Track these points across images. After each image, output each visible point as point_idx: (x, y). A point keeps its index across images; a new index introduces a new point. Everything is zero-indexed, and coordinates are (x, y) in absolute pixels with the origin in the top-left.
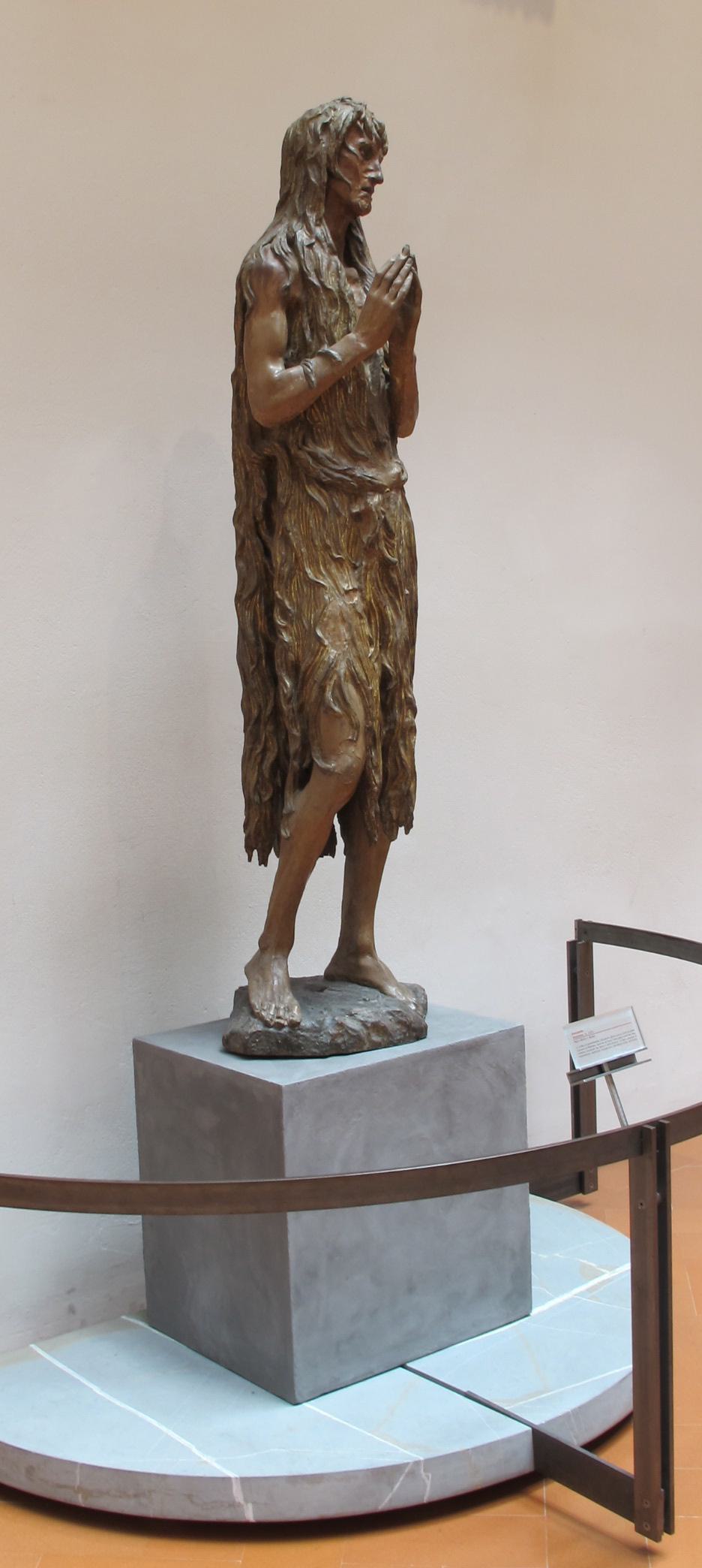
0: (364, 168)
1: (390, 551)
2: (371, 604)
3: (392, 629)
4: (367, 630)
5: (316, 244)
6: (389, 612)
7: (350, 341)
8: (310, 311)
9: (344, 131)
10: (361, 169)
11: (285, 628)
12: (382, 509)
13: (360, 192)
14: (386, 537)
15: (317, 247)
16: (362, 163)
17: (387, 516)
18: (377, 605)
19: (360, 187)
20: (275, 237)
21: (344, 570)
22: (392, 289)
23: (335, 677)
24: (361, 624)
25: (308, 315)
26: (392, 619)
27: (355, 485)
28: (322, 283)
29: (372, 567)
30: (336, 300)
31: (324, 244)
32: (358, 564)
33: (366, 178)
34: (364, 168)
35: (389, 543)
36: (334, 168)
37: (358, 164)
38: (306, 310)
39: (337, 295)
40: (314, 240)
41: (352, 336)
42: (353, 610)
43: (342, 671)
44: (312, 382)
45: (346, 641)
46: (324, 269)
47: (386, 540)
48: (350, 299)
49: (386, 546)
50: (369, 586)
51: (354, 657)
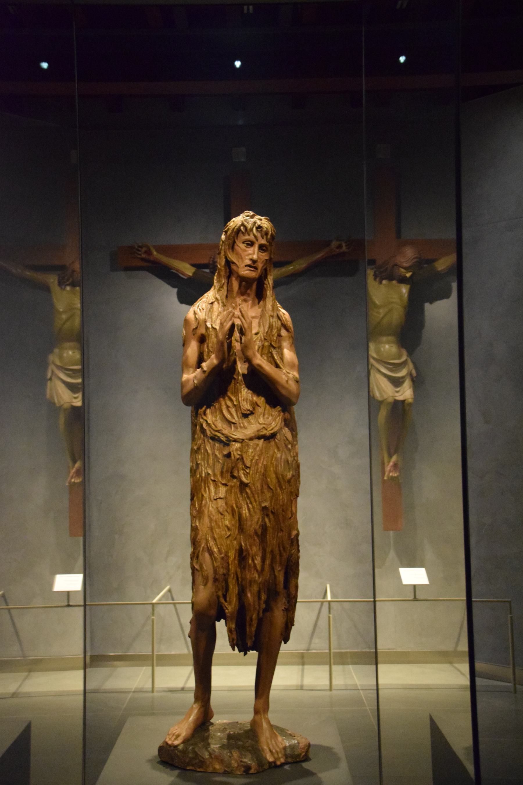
0: (246, 253)
1: (246, 476)
2: (232, 507)
4: (227, 523)
5: (216, 303)
6: (244, 512)
10: (243, 254)
11: (195, 517)
12: (239, 453)
14: (244, 468)
16: (245, 251)
17: (244, 456)
18: (237, 507)
19: (244, 265)
21: (217, 487)
23: (199, 549)
24: (221, 519)
29: (234, 486)
31: (220, 302)
32: (228, 484)
34: (246, 253)
35: (246, 471)
43: (203, 545)
46: (214, 317)
47: (243, 470)
49: (244, 474)
50: (233, 495)
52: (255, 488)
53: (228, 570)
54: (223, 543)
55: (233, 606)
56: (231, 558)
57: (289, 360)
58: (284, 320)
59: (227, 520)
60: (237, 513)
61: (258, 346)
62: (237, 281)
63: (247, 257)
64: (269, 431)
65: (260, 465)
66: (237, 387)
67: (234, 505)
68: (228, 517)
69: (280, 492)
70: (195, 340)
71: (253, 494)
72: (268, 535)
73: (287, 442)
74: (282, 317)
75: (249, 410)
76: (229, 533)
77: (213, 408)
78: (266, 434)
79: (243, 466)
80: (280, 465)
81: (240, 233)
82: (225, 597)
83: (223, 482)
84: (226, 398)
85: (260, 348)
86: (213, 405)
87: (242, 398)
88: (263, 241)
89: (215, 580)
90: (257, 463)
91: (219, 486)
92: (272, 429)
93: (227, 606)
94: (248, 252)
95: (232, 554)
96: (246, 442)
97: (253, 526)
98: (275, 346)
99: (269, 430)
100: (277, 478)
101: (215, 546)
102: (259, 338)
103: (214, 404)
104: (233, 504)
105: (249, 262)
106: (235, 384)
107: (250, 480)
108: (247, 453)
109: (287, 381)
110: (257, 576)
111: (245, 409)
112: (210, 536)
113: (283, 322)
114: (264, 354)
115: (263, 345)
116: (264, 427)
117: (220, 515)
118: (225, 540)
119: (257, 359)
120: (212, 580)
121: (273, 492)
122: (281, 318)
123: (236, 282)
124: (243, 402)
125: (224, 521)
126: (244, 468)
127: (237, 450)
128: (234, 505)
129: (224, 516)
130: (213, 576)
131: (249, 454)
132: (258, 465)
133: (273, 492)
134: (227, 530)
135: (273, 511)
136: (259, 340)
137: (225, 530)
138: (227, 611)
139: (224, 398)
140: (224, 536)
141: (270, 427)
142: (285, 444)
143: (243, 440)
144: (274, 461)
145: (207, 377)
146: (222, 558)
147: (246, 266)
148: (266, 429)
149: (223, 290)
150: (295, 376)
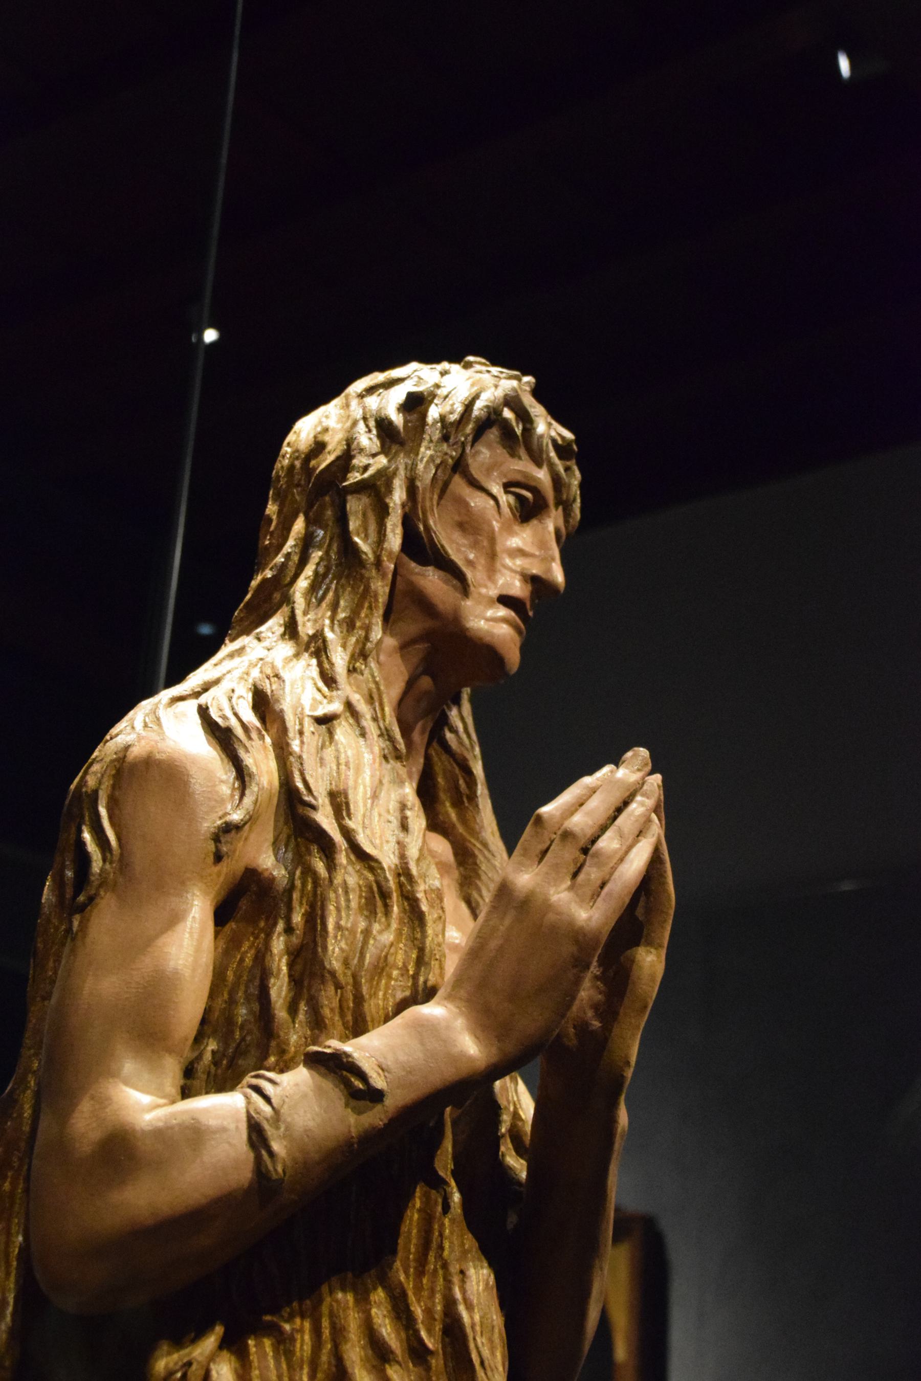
7: (424, 1028)
8: (297, 918)
15: (343, 732)
19: (494, 592)
20: (217, 682)
22: (591, 873)
25: (289, 930)
28: (347, 834)
30: (385, 895)
37: (496, 525)
38: (283, 912)
39: (392, 884)
40: (336, 707)
41: (433, 1010)
44: (271, 1154)
48: (432, 906)
62: (402, 656)
63: (508, 562)
66: (441, 1235)
70: (212, 896)
77: (267, 1343)
81: (493, 434)
84: (379, 1295)
86: (274, 1331)
87: (477, 1317)
103: (287, 1327)
105: (517, 588)
106: (428, 1220)
123: (398, 660)
124: (479, 1340)
139: (363, 1301)
145: (370, 1138)
149: (367, 672)
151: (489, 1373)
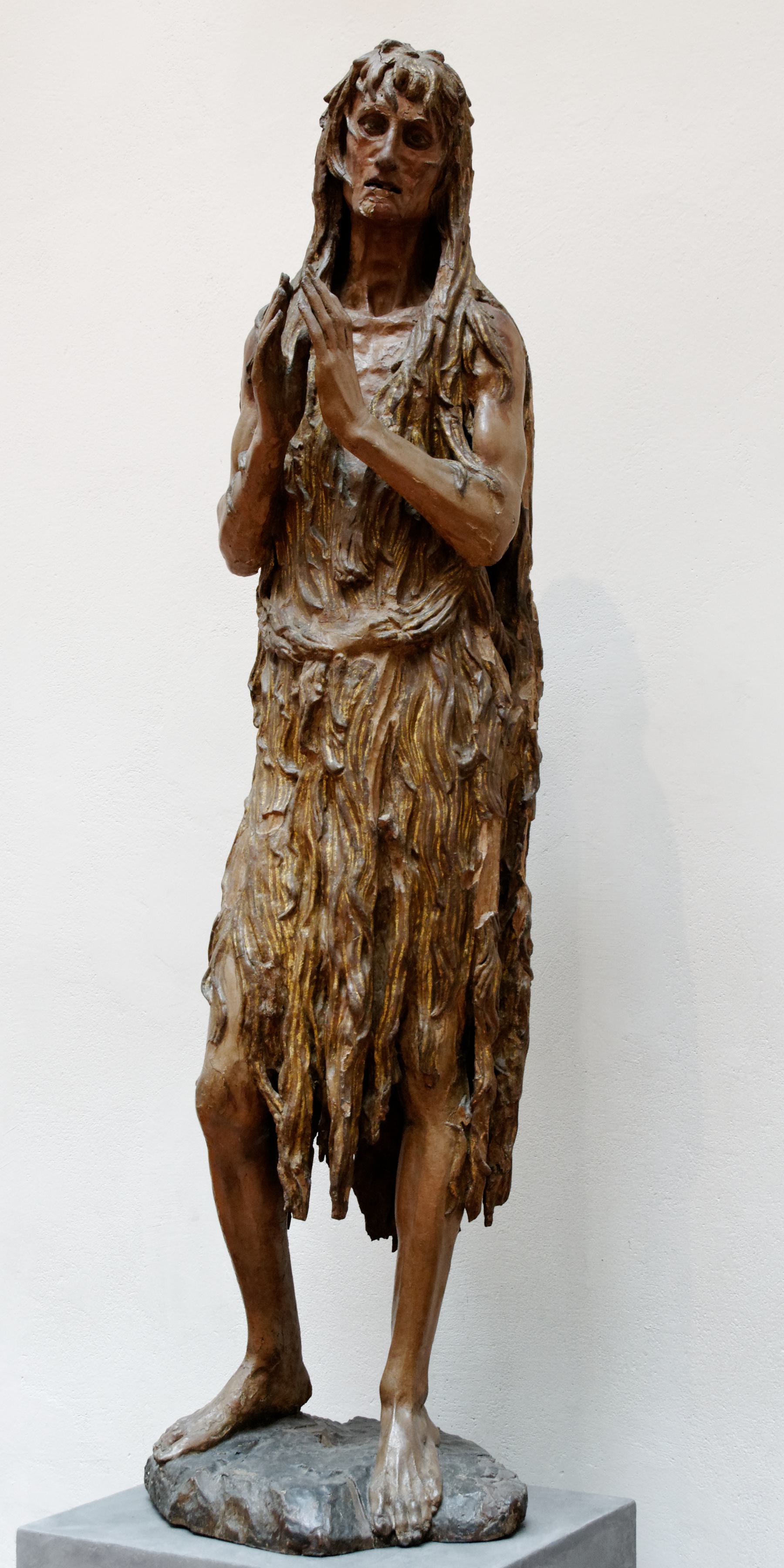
0: (369, 149)
3: (330, 877)
4: (288, 878)
6: (329, 849)
9: (340, 100)
12: (319, 688)
13: (363, 188)
14: (333, 731)
19: (363, 181)
24: (273, 867)
26: (332, 861)
27: (286, 652)
33: (371, 164)
36: (332, 164)
42: (264, 845)
45: (240, 891)
51: (243, 915)
52: (358, 786)
53: (280, 1003)
54: (272, 932)
55: (294, 1102)
56: (295, 972)
57: (484, 437)
58: (483, 331)
59: (287, 870)
60: (314, 852)
61: (394, 398)
63: (371, 160)
64: (406, 630)
65: (376, 721)
67: (309, 832)
68: (291, 863)
69: (437, 800)
71: (352, 802)
72: (397, 915)
73: (472, 664)
74: (476, 321)
75: (351, 572)
76: (289, 907)
78: (396, 637)
79: (332, 727)
80: (435, 724)
82: (273, 1078)
83: (288, 770)
85: (399, 408)
88: (416, 114)
89: (244, 1028)
90: (366, 718)
91: (278, 780)
92: (420, 625)
93: (277, 1103)
94: (373, 144)
95: (295, 963)
96: (338, 658)
97: (347, 889)
98: (447, 400)
99: (406, 627)
100: (428, 759)
101: (250, 940)
102: (400, 378)
104: (306, 828)
107: (345, 762)
108: (341, 687)
109: (462, 491)
110: (349, 1023)
111: (343, 570)
112: (241, 912)
113: (479, 337)
114: (411, 423)
115: (408, 398)
116: (391, 620)
117: (271, 856)
118: (278, 925)
119: (360, 426)
120: (238, 1027)
121: (416, 800)
122: (474, 326)
125: (281, 872)
126: (333, 731)
127: (311, 680)
128: (309, 832)
129: (282, 860)
130: (239, 1020)
131: (345, 691)
132: (370, 722)
133: (416, 800)
134: (285, 898)
135: (417, 851)
136: (397, 384)
137: (281, 898)
138: (276, 1116)
140: (277, 915)
141: (412, 619)
142: (464, 668)
143: (332, 653)
144: (422, 714)
146: (268, 972)
147: (368, 184)
148: (398, 626)
150: (491, 479)
151: (340, 563)
